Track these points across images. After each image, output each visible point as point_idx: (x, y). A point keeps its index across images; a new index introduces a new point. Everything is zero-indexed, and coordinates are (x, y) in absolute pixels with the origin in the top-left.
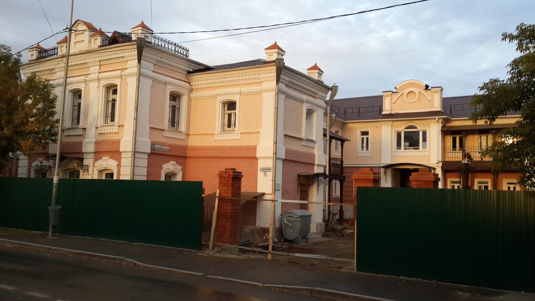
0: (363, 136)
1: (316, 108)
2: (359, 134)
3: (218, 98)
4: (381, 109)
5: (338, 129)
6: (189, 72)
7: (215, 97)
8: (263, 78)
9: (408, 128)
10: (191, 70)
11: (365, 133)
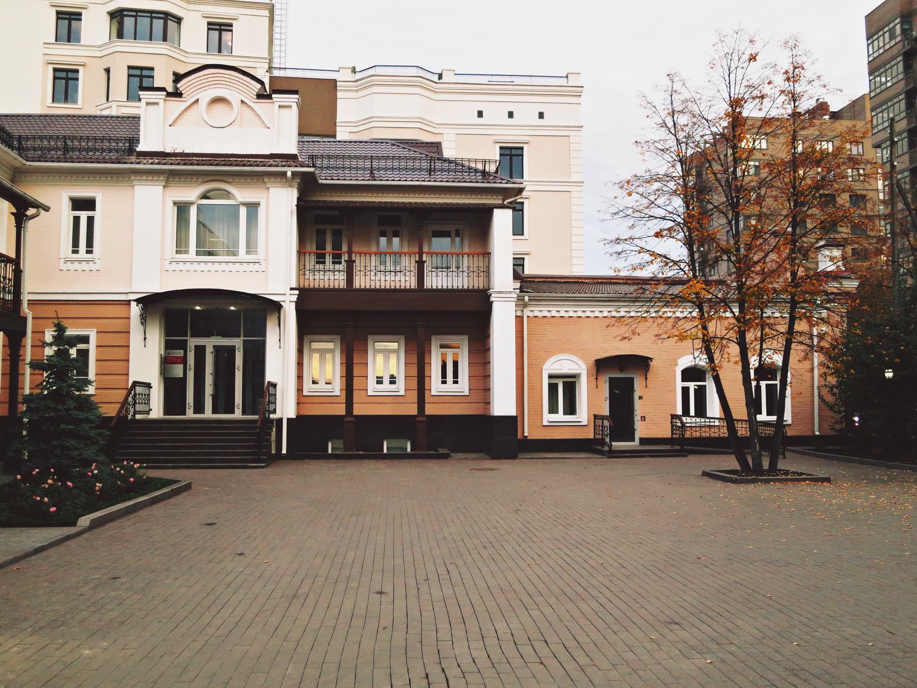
0: (77, 213)
2: (66, 205)
11: (87, 204)
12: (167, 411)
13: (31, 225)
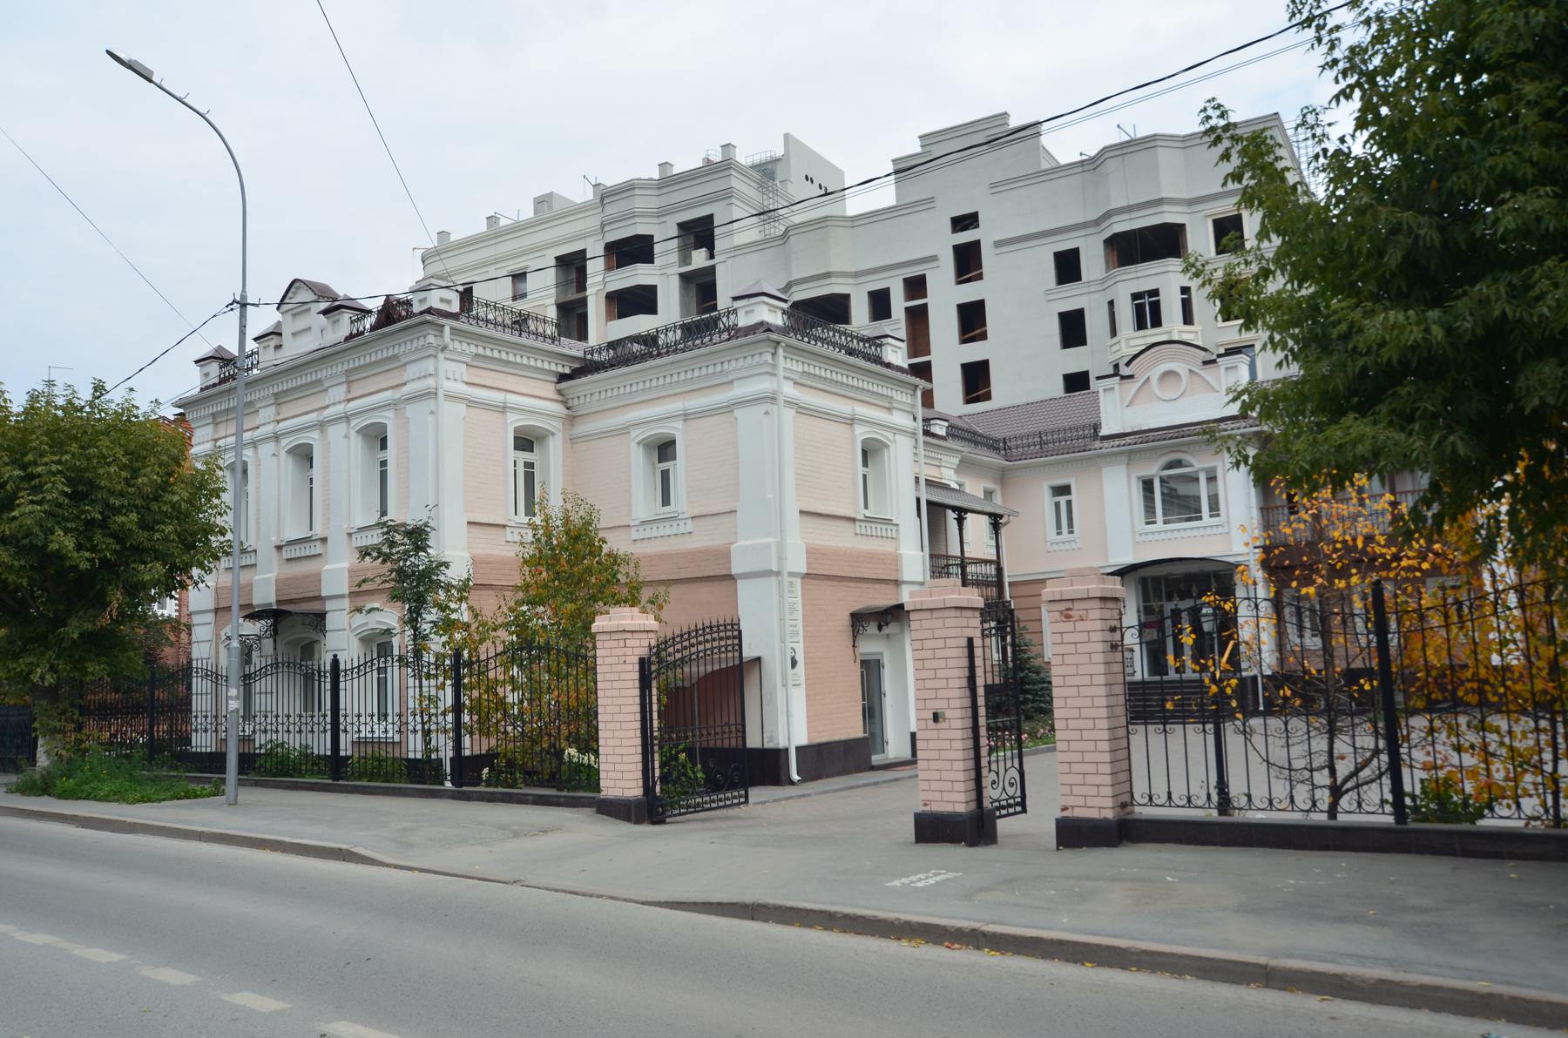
1: (890, 436)
2: (1047, 493)
3: (634, 434)
4: (1096, 427)
5: (990, 486)
6: (563, 378)
7: (625, 430)
8: (735, 370)
9: (1170, 466)
10: (567, 371)
11: (1064, 490)
12: (1153, 672)
13: (1003, 531)
